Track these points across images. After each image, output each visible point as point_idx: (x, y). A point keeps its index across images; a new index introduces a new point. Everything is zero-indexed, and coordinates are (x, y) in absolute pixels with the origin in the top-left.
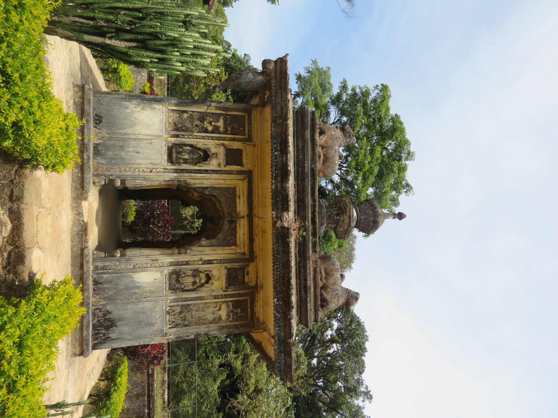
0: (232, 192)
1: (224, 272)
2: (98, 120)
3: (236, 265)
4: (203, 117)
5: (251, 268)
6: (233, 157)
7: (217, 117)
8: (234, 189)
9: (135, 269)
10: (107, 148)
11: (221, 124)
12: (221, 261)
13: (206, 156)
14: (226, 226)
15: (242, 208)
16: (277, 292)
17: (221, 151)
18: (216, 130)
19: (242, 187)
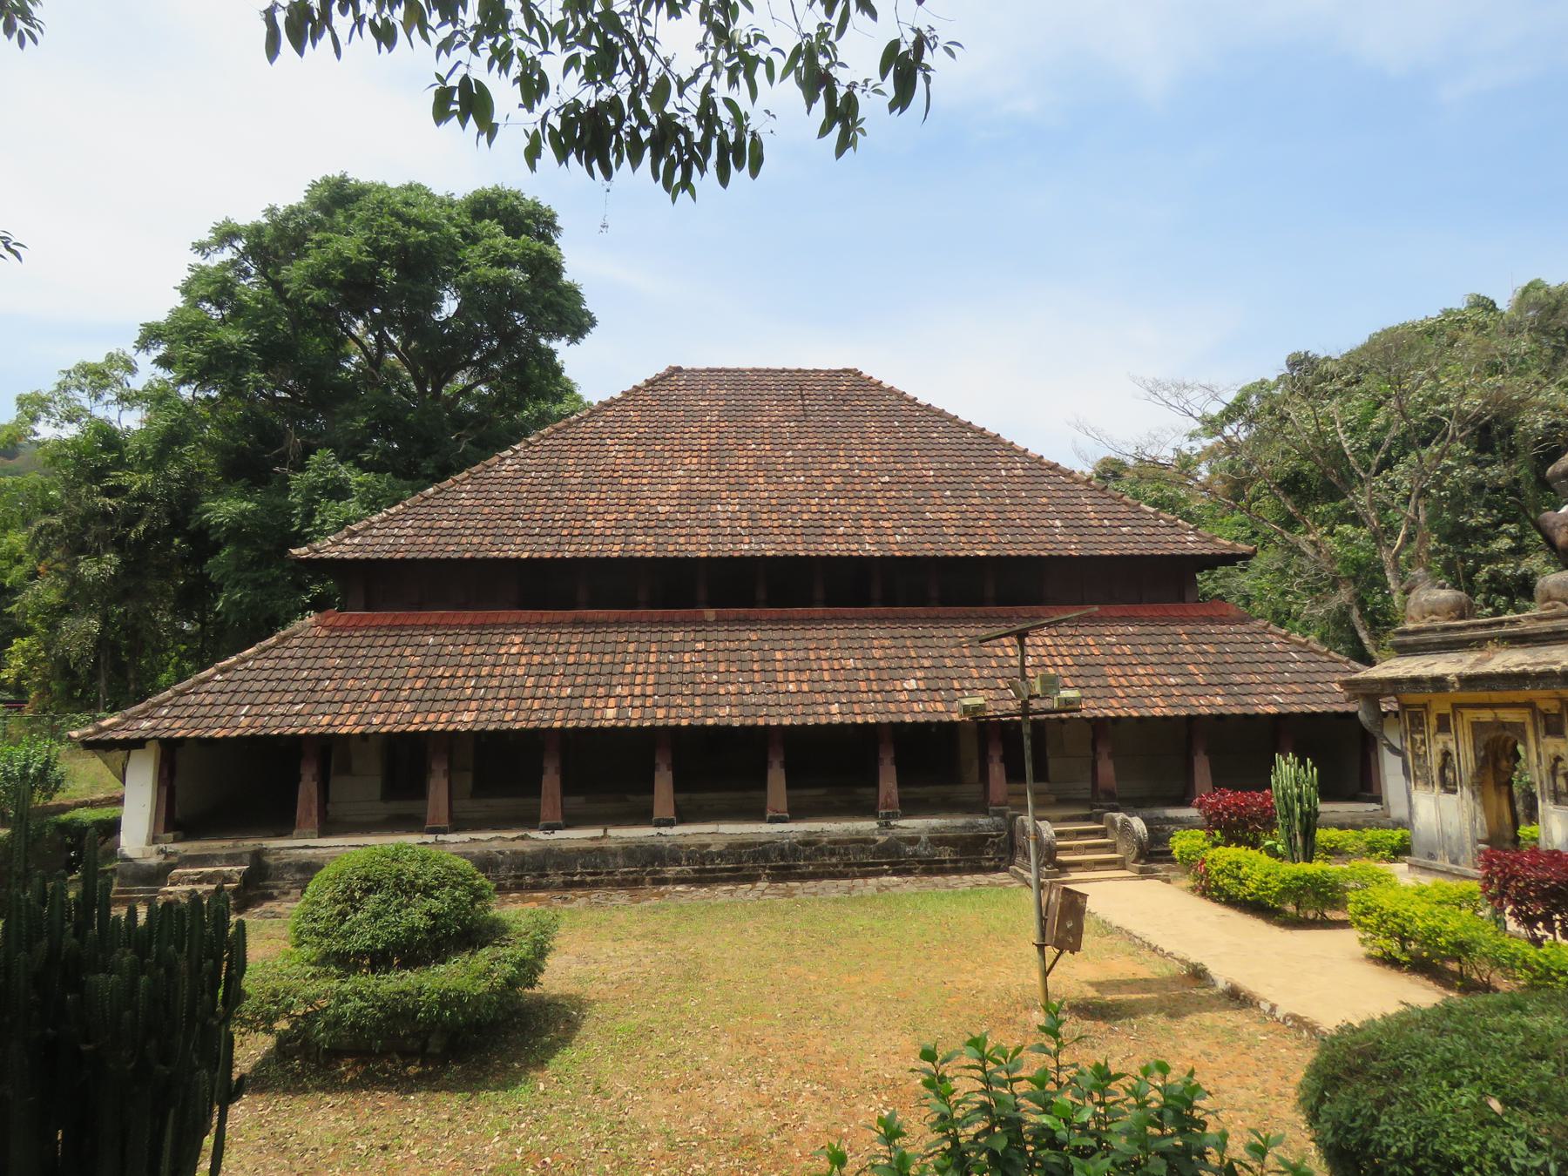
0: (1477, 727)
1: (1549, 740)
2: (1431, 856)
3: (1541, 725)
4: (1416, 756)
5: (1542, 706)
6: (1444, 725)
7: (1413, 741)
8: (1473, 723)
9: (1551, 841)
10: (1450, 853)
11: (1418, 737)
12: (1537, 742)
13: (1446, 754)
14: (1508, 733)
15: (1486, 716)
16: (1519, 688)
17: (1441, 737)
18: (1423, 742)
19: (1470, 715)
